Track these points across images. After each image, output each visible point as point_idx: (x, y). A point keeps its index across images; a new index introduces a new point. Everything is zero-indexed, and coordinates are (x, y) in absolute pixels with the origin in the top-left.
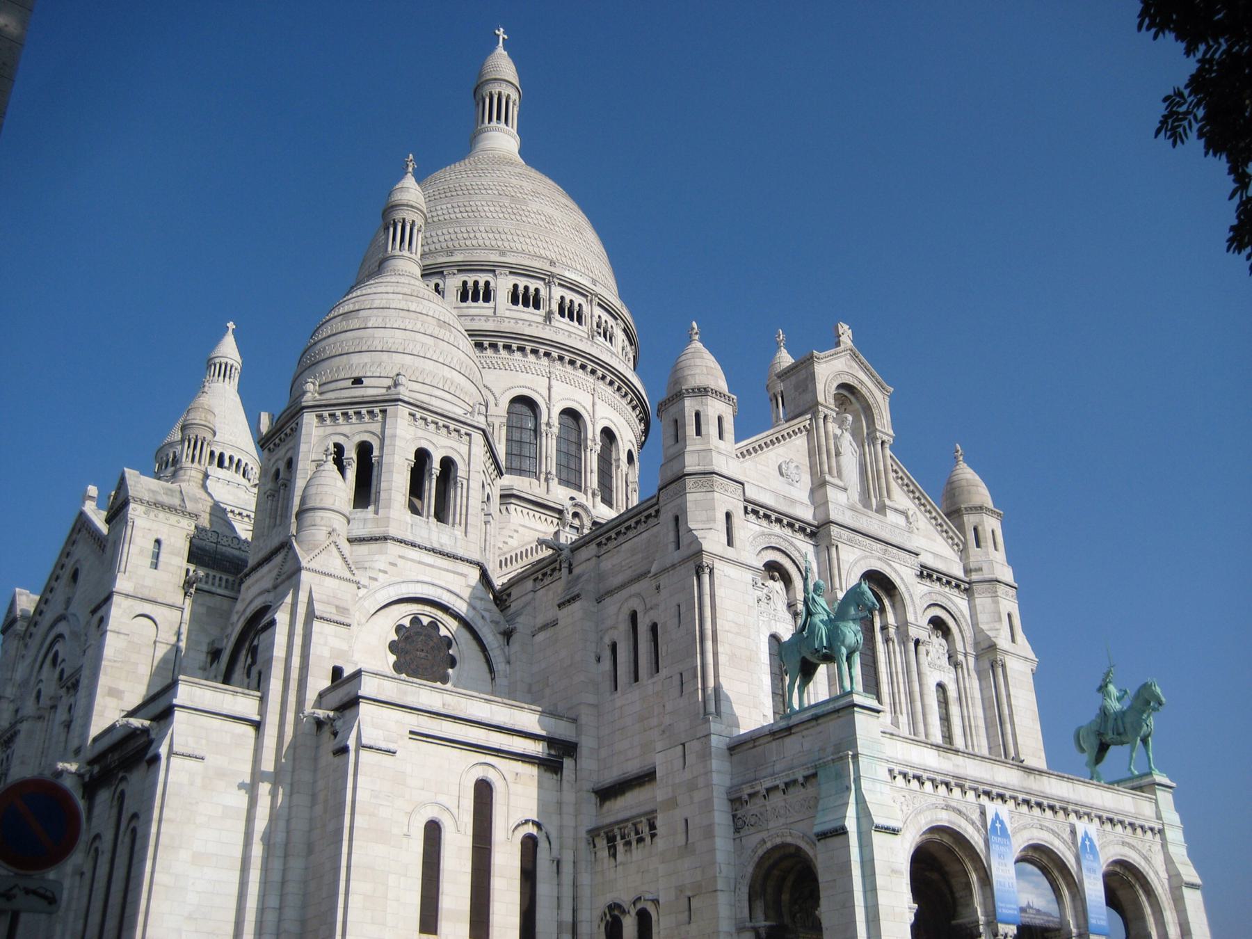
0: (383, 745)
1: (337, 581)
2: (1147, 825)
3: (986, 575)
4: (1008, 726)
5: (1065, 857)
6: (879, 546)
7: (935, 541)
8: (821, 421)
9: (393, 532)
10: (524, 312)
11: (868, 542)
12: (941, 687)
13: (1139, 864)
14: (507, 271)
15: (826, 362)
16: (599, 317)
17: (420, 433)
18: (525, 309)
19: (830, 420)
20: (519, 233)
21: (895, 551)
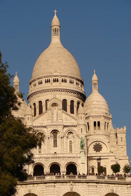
2: (77, 157)
6: (56, 126)
7: (72, 120)
11: (53, 126)
16: (62, 79)
19: (50, 110)
21: (59, 126)
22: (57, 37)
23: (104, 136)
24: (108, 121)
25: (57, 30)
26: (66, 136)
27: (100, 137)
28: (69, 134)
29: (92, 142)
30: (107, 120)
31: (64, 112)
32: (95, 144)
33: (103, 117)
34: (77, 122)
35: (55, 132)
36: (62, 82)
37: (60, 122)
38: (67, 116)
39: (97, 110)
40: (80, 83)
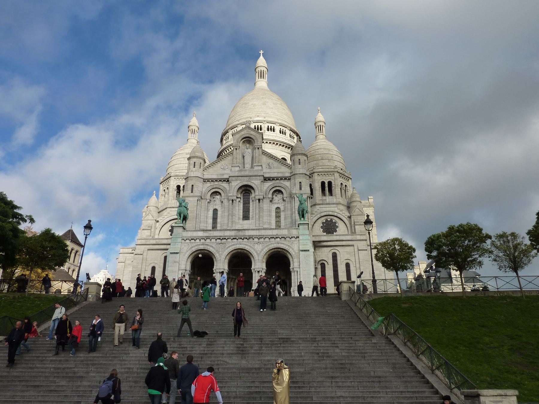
0: (139, 253)
4: (294, 215)
6: (248, 178)
8: (235, 150)
9: (169, 206)
16: (268, 126)
17: (177, 182)
21: (254, 177)
22: (263, 81)
24: (345, 181)
25: (263, 72)
27: (333, 208)
28: (275, 194)
29: (319, 216)
30: (343, 180)
32: (324, 221)
33: (337, 175)
34: (290, 171)
35: (246, 190)
39: (326, 162)
40: (295, 136)
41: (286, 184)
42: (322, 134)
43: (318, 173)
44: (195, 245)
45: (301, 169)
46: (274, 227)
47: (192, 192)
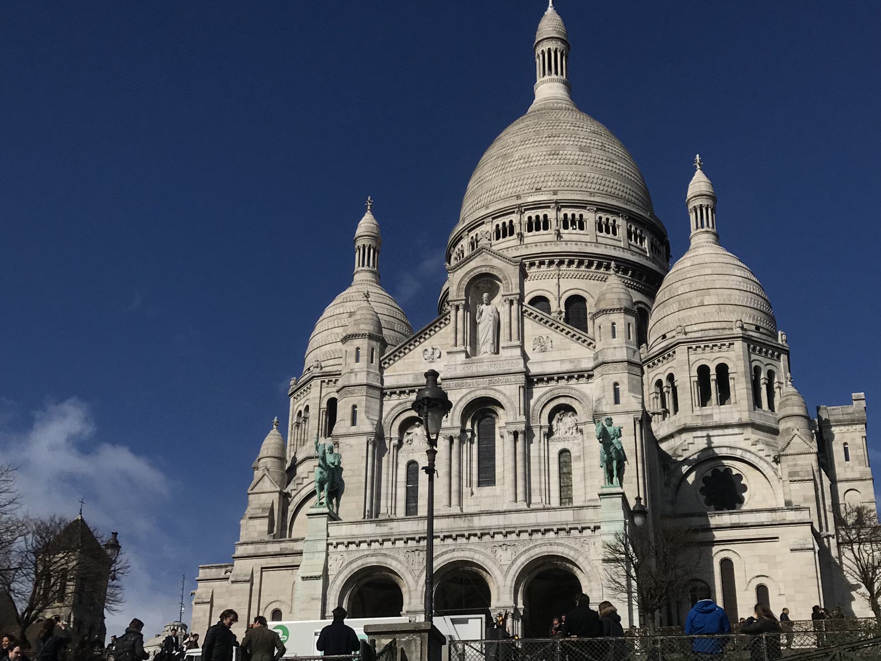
1: (268, 494)
2: (579, 527)
3: (600, 359)
5: (485, 565)
6: (487, 379)
7: (570, 349)
10: (502, 242)
11: (475, 380)
12: (564, 452)
13: (568, 555)
14: (490, 219)
15: (460, 268)
16: (565, 215)
17: (330, 390)
18: (504, 240)
20: (503, 183)
21: (501, 378)
22: (552, 81)
23: (750, 430)
24: (769, 361)
26: (541, 427)
28: (558, 415)
31: (530, 311)
32: (709, 474)
36: (565, 227)
37: (512, 358)
38: (545, 331)
39: (713, 313)
41: (583, 390)
42: (707, 232)
43: (690, 345)
44: (358, 555)
45: (617, 350)
46: (555, 502)
47: (354, 423)
